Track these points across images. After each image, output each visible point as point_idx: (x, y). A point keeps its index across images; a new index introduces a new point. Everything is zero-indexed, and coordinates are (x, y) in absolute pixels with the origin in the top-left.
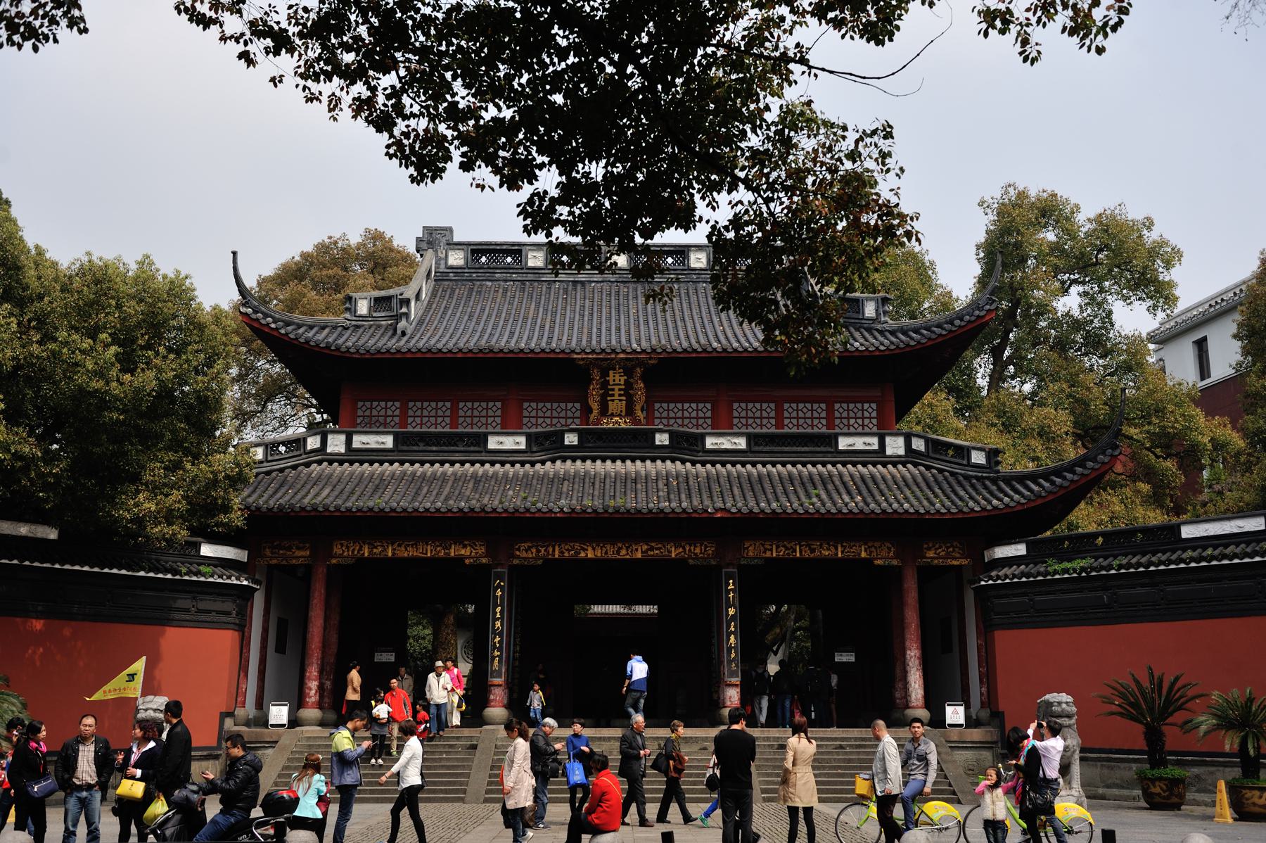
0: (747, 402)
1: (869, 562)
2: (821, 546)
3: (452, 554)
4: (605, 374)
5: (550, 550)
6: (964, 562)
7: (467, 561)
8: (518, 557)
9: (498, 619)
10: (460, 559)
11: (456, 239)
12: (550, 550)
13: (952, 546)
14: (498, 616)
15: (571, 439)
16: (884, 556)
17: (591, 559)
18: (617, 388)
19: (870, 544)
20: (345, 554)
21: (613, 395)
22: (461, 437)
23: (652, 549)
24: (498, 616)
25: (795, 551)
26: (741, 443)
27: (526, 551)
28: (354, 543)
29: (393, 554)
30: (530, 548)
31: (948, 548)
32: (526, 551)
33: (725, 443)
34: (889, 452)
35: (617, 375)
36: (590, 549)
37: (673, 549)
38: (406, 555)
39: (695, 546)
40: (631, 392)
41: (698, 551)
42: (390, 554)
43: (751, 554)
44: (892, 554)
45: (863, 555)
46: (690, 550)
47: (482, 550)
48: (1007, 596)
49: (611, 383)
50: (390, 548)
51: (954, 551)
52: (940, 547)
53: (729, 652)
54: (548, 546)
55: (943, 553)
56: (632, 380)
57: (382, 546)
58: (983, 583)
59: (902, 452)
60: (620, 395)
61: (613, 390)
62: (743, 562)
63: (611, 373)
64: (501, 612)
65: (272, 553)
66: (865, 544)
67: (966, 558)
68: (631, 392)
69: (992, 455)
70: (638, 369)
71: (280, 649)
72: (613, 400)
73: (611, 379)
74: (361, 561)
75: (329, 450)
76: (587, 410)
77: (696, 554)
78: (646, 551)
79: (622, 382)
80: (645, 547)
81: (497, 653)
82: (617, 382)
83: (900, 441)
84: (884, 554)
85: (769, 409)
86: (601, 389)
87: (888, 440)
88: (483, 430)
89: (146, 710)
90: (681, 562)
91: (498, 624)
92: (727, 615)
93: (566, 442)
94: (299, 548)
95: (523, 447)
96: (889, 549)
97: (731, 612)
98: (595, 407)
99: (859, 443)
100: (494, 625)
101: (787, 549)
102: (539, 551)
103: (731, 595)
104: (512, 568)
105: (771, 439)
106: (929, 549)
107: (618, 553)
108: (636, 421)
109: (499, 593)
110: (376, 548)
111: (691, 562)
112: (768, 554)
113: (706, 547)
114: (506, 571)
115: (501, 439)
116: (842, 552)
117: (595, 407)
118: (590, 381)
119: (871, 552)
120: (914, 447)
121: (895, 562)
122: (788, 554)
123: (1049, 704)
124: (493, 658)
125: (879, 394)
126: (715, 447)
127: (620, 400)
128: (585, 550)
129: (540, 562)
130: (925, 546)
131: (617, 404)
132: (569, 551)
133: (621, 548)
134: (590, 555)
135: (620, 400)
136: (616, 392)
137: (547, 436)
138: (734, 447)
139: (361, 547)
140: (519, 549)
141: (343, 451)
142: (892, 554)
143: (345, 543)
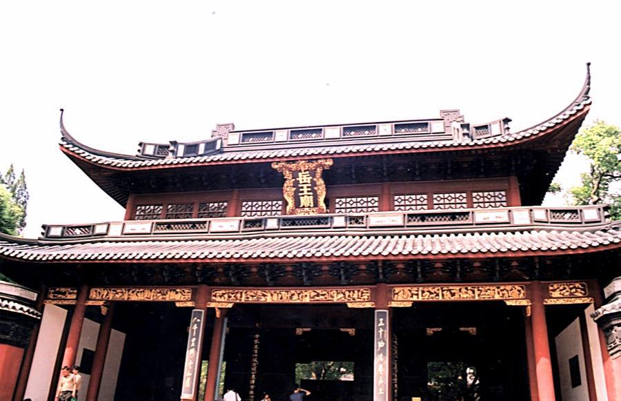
4: (295, 174)
6: (587, 300)
7: (178, 305)
10: (173, 303)
12: (239, 295)
13: (574, 287)
15: (272, 224)
18: (305, 186)
19: (502, 288)
20: (97, 298)
21: (303, 192)
23: (318, 295)
24: (193, 345)
25: (438, 295)
26: (399, 221)
27: (221, 297)
29: (128, 298)
30: (223, 294)
31: (571, 289)
32: (221, 297)
35: (305, 176)
36: (269, 295)
40: (316, 188)
41: (355, 296)
42: (126, 299)
43: (400, 298)
44: (522, 295)
45: (497, 297)
46: (349, 296)
49: (301, 182)
51: (576, 291)
52: (565, 288)
54: (237, 293)
55: (567, 294)
56: (315, 179)
57: (122, 293)
60: (308, 191)
61: (302, 188)
62: (394, 305)
63: (300, 174)
64: (196, 342)
65: (54, 296)
66: (498, 288)
67: (588, 297)
68: (316, 188)
70: (318, 169)
72: (303, 196)
77: (354, 299)
78: (313, 297)
79: (309, 182)
82: (305, 181)
84: (515, 294)
86: (294, 187)
94: (70, 293)
96: (519, 291)
97: (381, 344)
101: (431, 293)
102: (229, 297)
103: (381, 330)
106: (554, 290)
107: (291, 298)
110: (117, 293)
111: (350, 305)
112: (415, 298)
113: (362, 293)
114: (203, 311)
116: (479, 295)
118: (286, 180)
119: (503, 294)
122: (432, 298)
127: (309, 195)
128: (264, 296)
130: (551, 288)
131: (306, 200)
132: (253, 296)
133: (293, 295)
134: (269, 299)
135: (309, 195)
136: (305, 190)
140: (215, 296)
142: (522, 295)
143: (98, 290)
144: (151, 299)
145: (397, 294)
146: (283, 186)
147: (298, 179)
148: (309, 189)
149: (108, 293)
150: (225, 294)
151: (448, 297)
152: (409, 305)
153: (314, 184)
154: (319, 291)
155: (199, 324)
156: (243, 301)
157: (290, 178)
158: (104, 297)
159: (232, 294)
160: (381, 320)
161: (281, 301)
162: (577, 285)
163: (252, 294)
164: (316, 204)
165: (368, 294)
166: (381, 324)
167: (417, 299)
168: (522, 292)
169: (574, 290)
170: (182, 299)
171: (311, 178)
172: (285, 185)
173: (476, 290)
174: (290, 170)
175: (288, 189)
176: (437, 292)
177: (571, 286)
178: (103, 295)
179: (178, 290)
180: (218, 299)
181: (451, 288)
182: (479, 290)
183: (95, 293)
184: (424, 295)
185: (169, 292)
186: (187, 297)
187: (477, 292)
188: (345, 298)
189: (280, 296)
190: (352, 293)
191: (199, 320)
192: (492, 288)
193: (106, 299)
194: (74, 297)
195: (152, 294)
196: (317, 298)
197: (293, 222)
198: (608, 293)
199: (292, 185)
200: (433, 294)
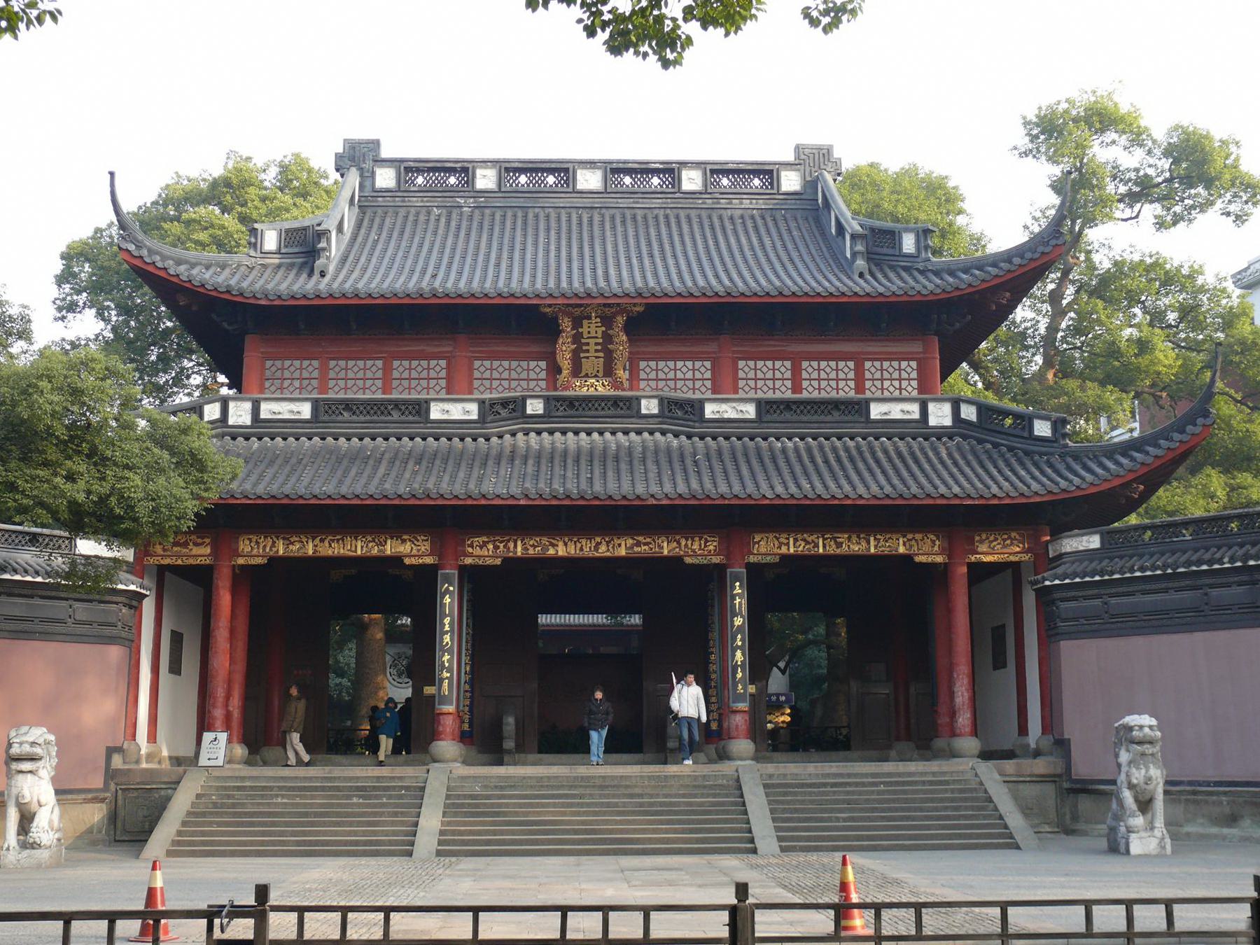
0: (755, 359)
1: (908, 558)
2: (849, 539)
3: (388, 552)
4: (577, 323)
5: (511, 545)
6: (1025, 557)
7: (407, 561)
8: (471, 555)
9: (447, 632)
10: (397, 560)
11: (385, 153)
12: (511, 545)
13: (1010, 538)
14: (447, 628)
15: (535, 407)
16: (928, 550)
17: (562, 558)
18: (592, 341)
19: (910, 536)
20: (255, 552)
21: (588, 351)
22: (397, 404)
23: (638, 544)
24: (447, 628)
25: (817, 546)
26: (750, 411)
27: (481, 547)
28: (265, 537)
30: (485, 544)
31: (1004, 540)
32: (481, 547)
33: (729, 411)
34: (933, 421)
36: (561, 544)
37: (665, 544)
38: (330, 553)
39: (693, 541)
41: (696, 546)
42: (310, 552)
43: (763, 550)
44: (936, 548)
45: (902, 550)
46: (686, 545)
47: (425, 546)
48: (1075, 599)
50: (311, 545)
51: (1012, 544)
52: (996, 539)
53: (735, 673)
56: (610, 332)
58: (1047, 583)
59: (948, 422)
60: (596, 351)
61: (588, 344)
62: (752, 559)
63: (585, 322)
64: (451, 624)
65: (164, 550)
69: (1059, 425)
71: (175, 668)
72: (588, 358)
73: (584, 330)
74: (274, 561)
75: (231, 422)
76: (554, 370)
77: (694, 551)
79: (599, 335)
80: (630, 542)
81: (446, 675)
83: (947, 408)
84: (926, 548)
85: (784, 367)
86: (574, 344)
87: (932, 407)
88: (423, 396)
89: (21, 744)
90: (676, 561)
91: (447, 638)
92: (733, 626)
93: (529, 411)
94: (196, 544)
95: (475, 417)
96: (933, 542)
98: (565, 364)
99: (896, 411)
100: (442, 640)
101: (807, 543)
102: (496, 548)
104: (463, 569)
105: (787, 405)
106: (981, 542)
108: (617, 385)
109: (447, 600)
110: (292, 543)
111: (688, 560)
112: (784, 550)
113: (706, 541)
115: (447, 406)
116: (876, 547)
117: (565, 364)
118: (560, 332)
119: (911, 546)
120: (963, 416)
121: (939, 559)
122: (809, 550)
123: (1130, 729)
124: (442, 680)
125: (921, 350)
126: (717, 416)
127: (596, 357)
128: (554, 545)
129: (498, 562)
131: (592, 362)
132: (533, 546)
133: (598, 544)
134: (562, 551)
136: (592, 348)
137: (505, 403)
138: (740, 416)
139: (274, 542)
140: (471, 546)
141: (249, 423)
142: (936, 548)
143: (254, 538)
144: (359, 552)
145: (758, 543)
146: (555, 342)
147: (580, 330)
148: (599, 347)
149: (274, 542)
150: (488, 542)
151: (832, 549)
152: (777, 559)
153: (608, 338)
154: (641, 538)
155: (451, 593)
156: (519, 554)
157: (569, 329)
158: (268, 550)
159: (501, 542)
160: (738, 584)
161: (579, 554)
162: (1013, 534)
163: (531, 543)
164: (609, 371)
165: (715, 544)
166: (738, 591)
167: (786, 551)
168: (937, 543)
169: (1008, 542)
170: (414, 552)
171: (604, 329)
172: (560, 341)
173: (872, 539)
174: (569, 315)
175: (564, 348)
176: (816, 540)
177: (1006, 536)
178: (265, 547)
179: (405, 537)
180: (477, 551)
181: (836, 535)
182: (875, 539)
183: (247, 542)
184: (798, 543)
185: (389, 542)
186: (423, 549)
187: (872, 543)
188: (680, 549)
189: (579, 545)
190: (689, 542)
191: (451, 588)
192: (894, 537)
193: (271, 553)
194: (208, 550)
195: (359, 544)
196: (637, 549)
197: (571, 402)
198: (1055, 551)
199: (569, 340)
200: (809, 543)
